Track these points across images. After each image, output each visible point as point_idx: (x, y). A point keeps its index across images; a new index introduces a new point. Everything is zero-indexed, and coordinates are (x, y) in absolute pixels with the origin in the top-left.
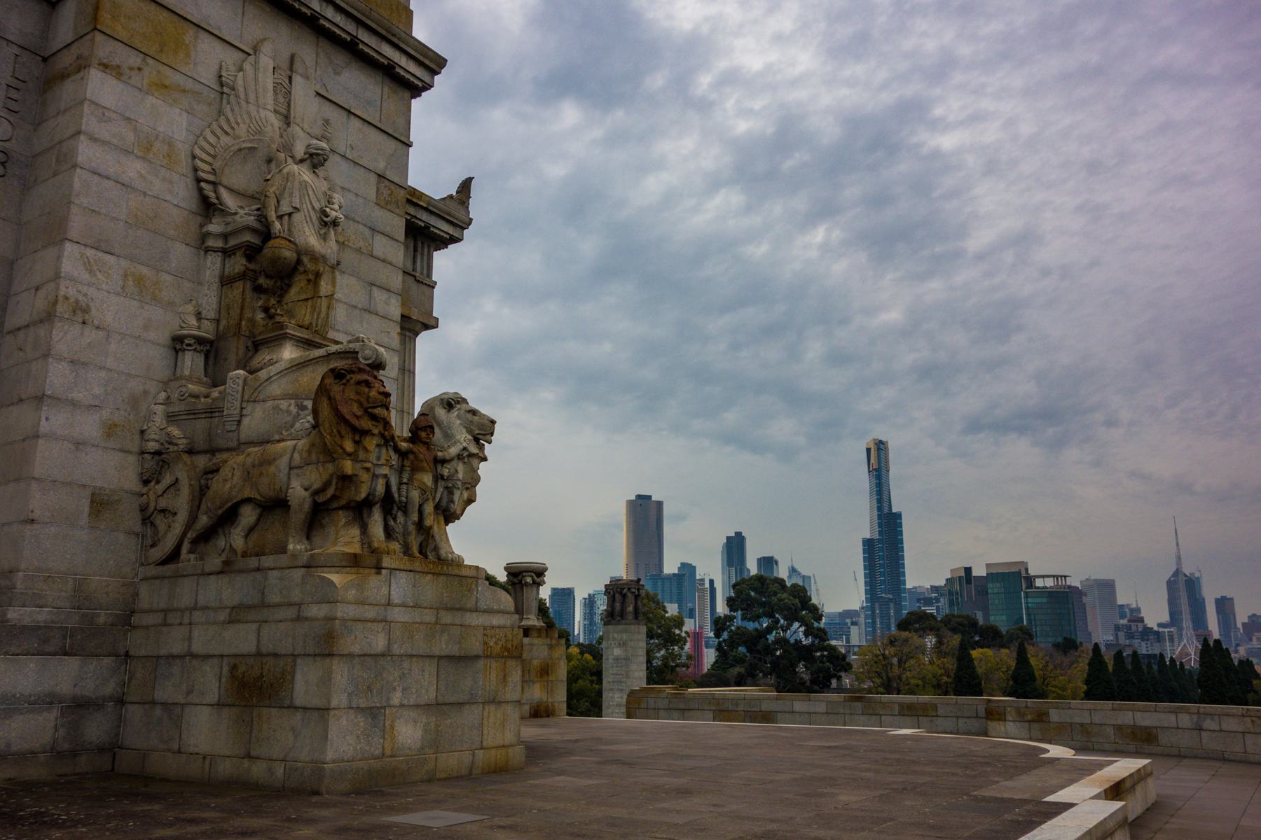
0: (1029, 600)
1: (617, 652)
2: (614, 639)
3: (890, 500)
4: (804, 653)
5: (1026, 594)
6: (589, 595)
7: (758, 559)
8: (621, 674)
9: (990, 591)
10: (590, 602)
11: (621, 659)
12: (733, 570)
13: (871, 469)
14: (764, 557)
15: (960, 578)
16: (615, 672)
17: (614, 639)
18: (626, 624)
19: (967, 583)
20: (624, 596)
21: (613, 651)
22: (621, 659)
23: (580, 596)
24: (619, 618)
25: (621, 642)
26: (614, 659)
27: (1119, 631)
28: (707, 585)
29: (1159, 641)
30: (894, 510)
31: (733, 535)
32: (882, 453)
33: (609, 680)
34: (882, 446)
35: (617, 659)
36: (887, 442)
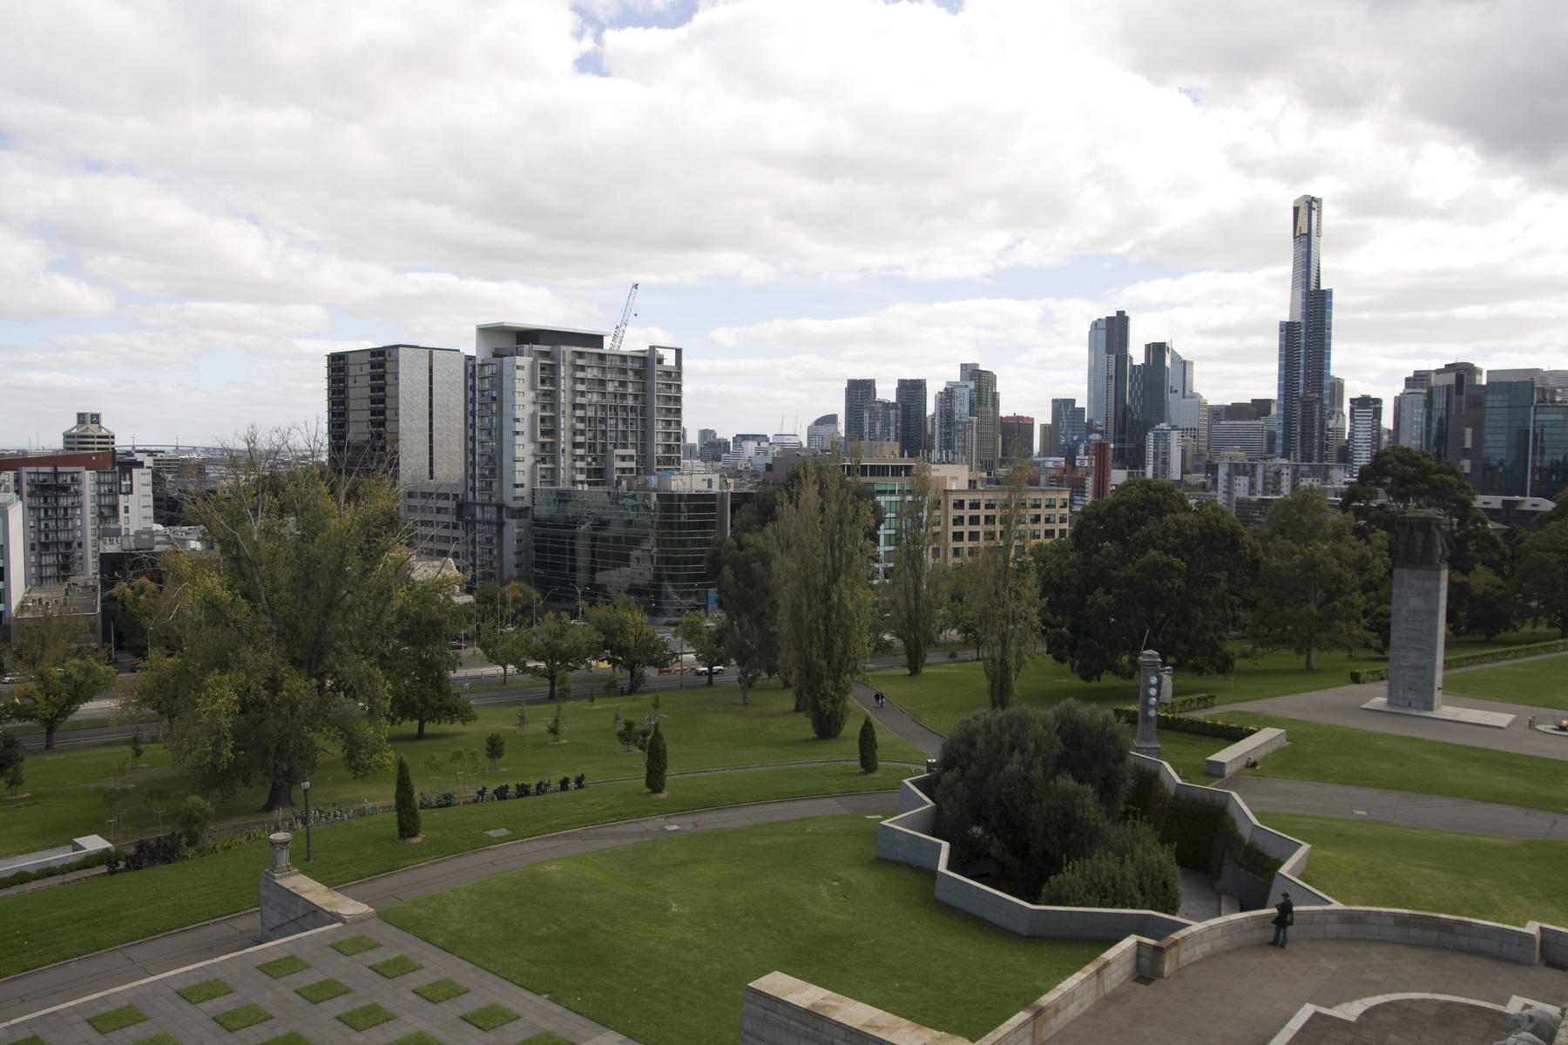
0: (1539, 417)
1: (1415, 602)
5: (1535, 407)
7: (1146, 345)
10: (948, 396)
13: (1298, 234)
14: (1154, 343)
15: (1449, 387)
19: (1457, 393)
20: (1428, 533)
30: (1322, 288)
31: (1115, 315)
32: (1314, 213)
36: (1321, 199)
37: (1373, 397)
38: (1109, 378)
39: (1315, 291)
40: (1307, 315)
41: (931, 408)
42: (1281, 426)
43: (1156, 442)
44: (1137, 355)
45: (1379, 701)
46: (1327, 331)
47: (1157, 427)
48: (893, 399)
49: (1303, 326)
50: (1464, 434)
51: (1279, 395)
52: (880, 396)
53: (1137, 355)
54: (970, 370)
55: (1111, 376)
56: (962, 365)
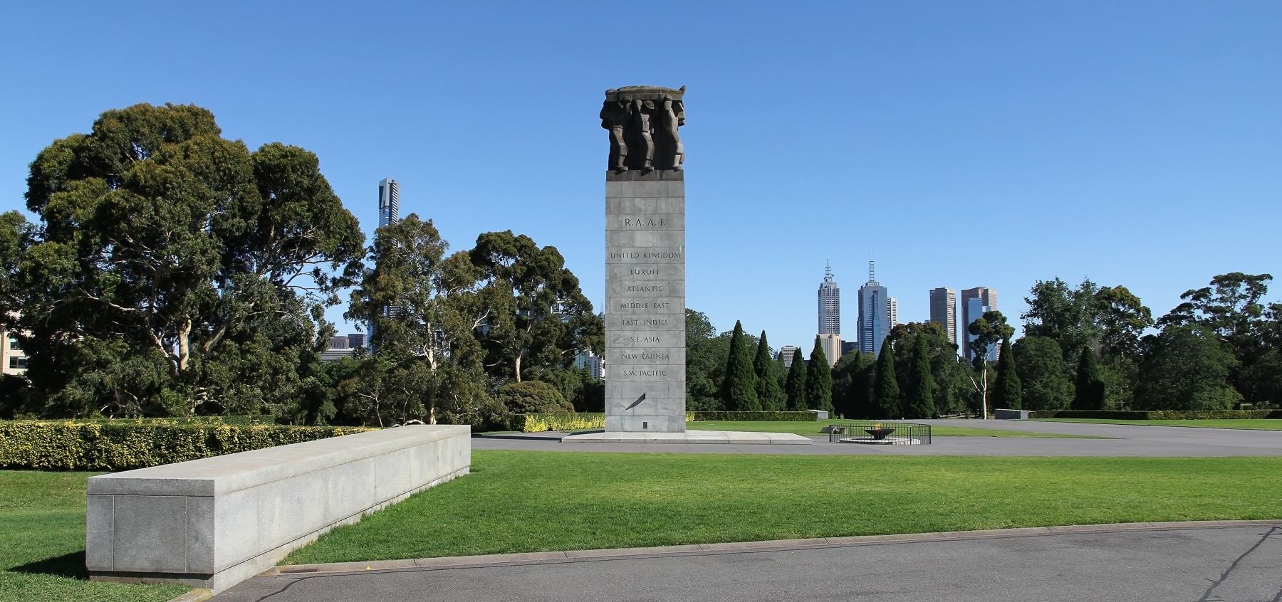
2: (636, 211)
13: (382, 206)
16: (638, 283)
17: (636, 211)
21: (632, 238)
25: (656, 219)
26: (637, 256)
33: (624, 301)
35: (644, 255)
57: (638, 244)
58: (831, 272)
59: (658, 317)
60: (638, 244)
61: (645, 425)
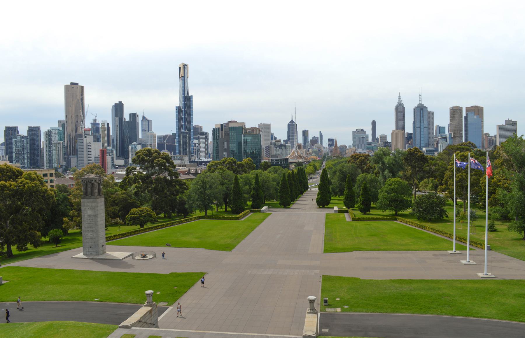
0: (245, 138)
1: (90, 212)
3: (188, 90)
4: (169, 183)
5: (244, 135)
6: (48, 130)
7: (129, 114)
8: (92, 223)
9: (230, 134)
10: (49, 134)
11: (92, 216)
12: (118, 118)
13: (181, 76)
14: (132, 113)
15: (219, 128)
16: (88, 222)
18: (94, 199)
19: (221, 131)
22: (92, 216)
23: (44, 130)
24: (90, 196)
25: (92, 208)
26: (88, 216)
27: (272, 145)
28: (106, 126)
29: (285, 149)
30: (189, 95)
31: (118, 103)
32: (186, 70)
33: (86, 226)
34: (186, 67)
36: (188, 65)
37: (205, 132)
38: (117, 126)
39: (187, 96)
40: (185, 104)
41: (43, 139)
42: (178, 143)
43: (132, 149)
44: (127, 118)
45: (81, 255)
46: (191, 110)
47: (132, 144)
48: (26, 134)
49: (184, 108)
50: (224, 144)
51: (176, 132)
52: (20, 133)
53: (127, 118)
54: (62, 123)
55: (117, 125)
56: (59, 121)
57: (88, 213)
58: (401, 99)
59: (93, 230)
60: (88, 213)
61: (91, 253)
